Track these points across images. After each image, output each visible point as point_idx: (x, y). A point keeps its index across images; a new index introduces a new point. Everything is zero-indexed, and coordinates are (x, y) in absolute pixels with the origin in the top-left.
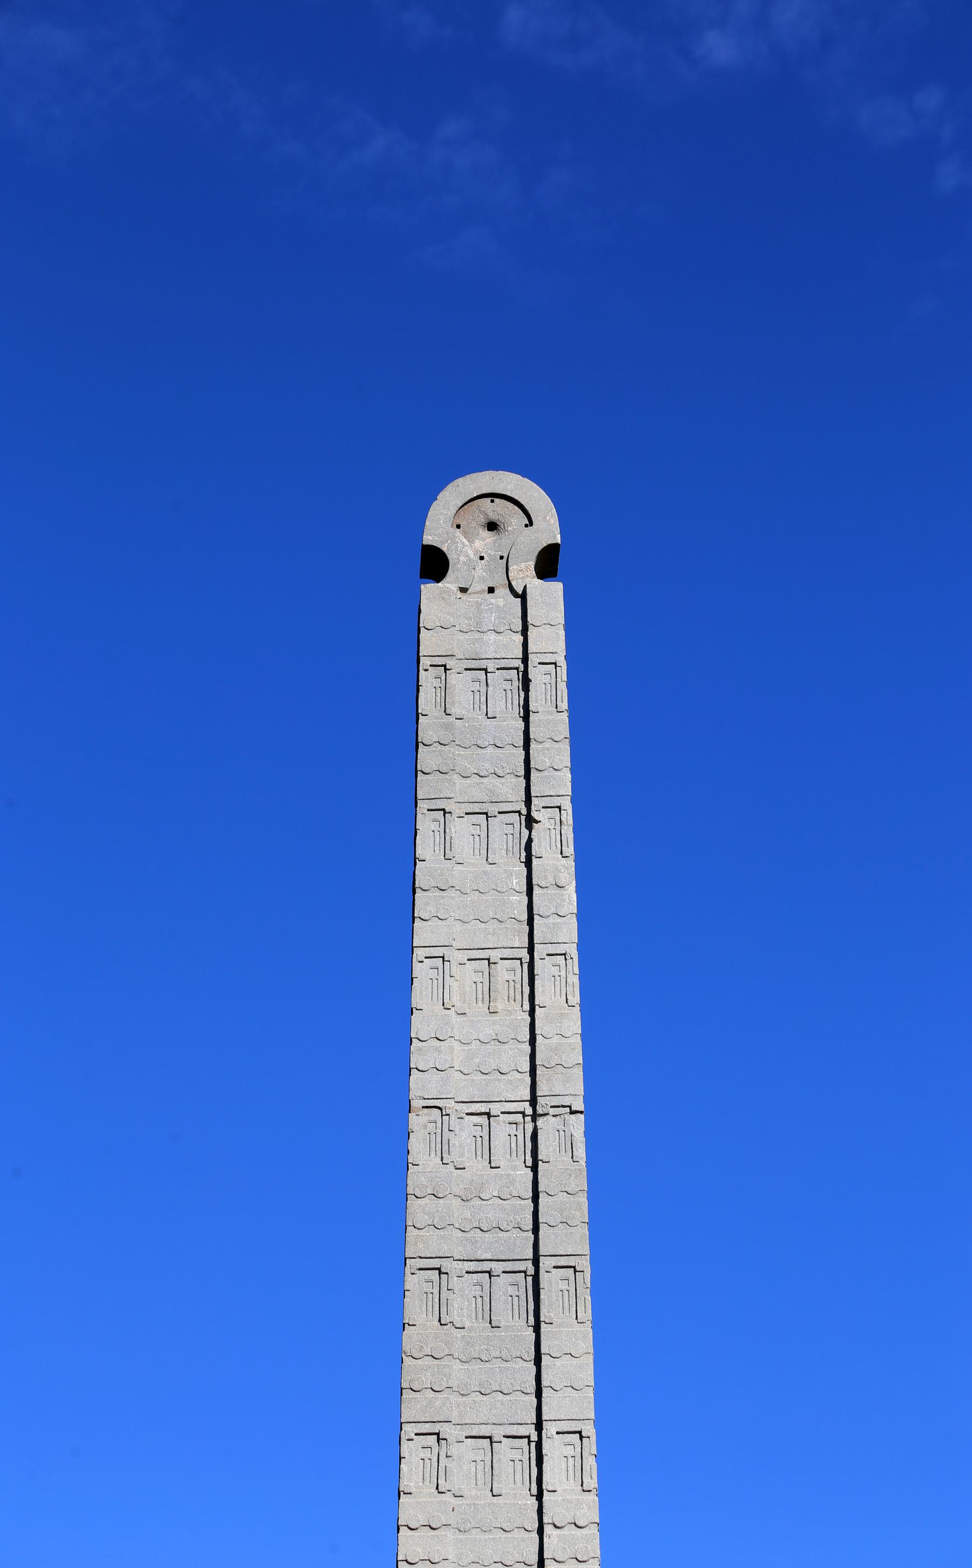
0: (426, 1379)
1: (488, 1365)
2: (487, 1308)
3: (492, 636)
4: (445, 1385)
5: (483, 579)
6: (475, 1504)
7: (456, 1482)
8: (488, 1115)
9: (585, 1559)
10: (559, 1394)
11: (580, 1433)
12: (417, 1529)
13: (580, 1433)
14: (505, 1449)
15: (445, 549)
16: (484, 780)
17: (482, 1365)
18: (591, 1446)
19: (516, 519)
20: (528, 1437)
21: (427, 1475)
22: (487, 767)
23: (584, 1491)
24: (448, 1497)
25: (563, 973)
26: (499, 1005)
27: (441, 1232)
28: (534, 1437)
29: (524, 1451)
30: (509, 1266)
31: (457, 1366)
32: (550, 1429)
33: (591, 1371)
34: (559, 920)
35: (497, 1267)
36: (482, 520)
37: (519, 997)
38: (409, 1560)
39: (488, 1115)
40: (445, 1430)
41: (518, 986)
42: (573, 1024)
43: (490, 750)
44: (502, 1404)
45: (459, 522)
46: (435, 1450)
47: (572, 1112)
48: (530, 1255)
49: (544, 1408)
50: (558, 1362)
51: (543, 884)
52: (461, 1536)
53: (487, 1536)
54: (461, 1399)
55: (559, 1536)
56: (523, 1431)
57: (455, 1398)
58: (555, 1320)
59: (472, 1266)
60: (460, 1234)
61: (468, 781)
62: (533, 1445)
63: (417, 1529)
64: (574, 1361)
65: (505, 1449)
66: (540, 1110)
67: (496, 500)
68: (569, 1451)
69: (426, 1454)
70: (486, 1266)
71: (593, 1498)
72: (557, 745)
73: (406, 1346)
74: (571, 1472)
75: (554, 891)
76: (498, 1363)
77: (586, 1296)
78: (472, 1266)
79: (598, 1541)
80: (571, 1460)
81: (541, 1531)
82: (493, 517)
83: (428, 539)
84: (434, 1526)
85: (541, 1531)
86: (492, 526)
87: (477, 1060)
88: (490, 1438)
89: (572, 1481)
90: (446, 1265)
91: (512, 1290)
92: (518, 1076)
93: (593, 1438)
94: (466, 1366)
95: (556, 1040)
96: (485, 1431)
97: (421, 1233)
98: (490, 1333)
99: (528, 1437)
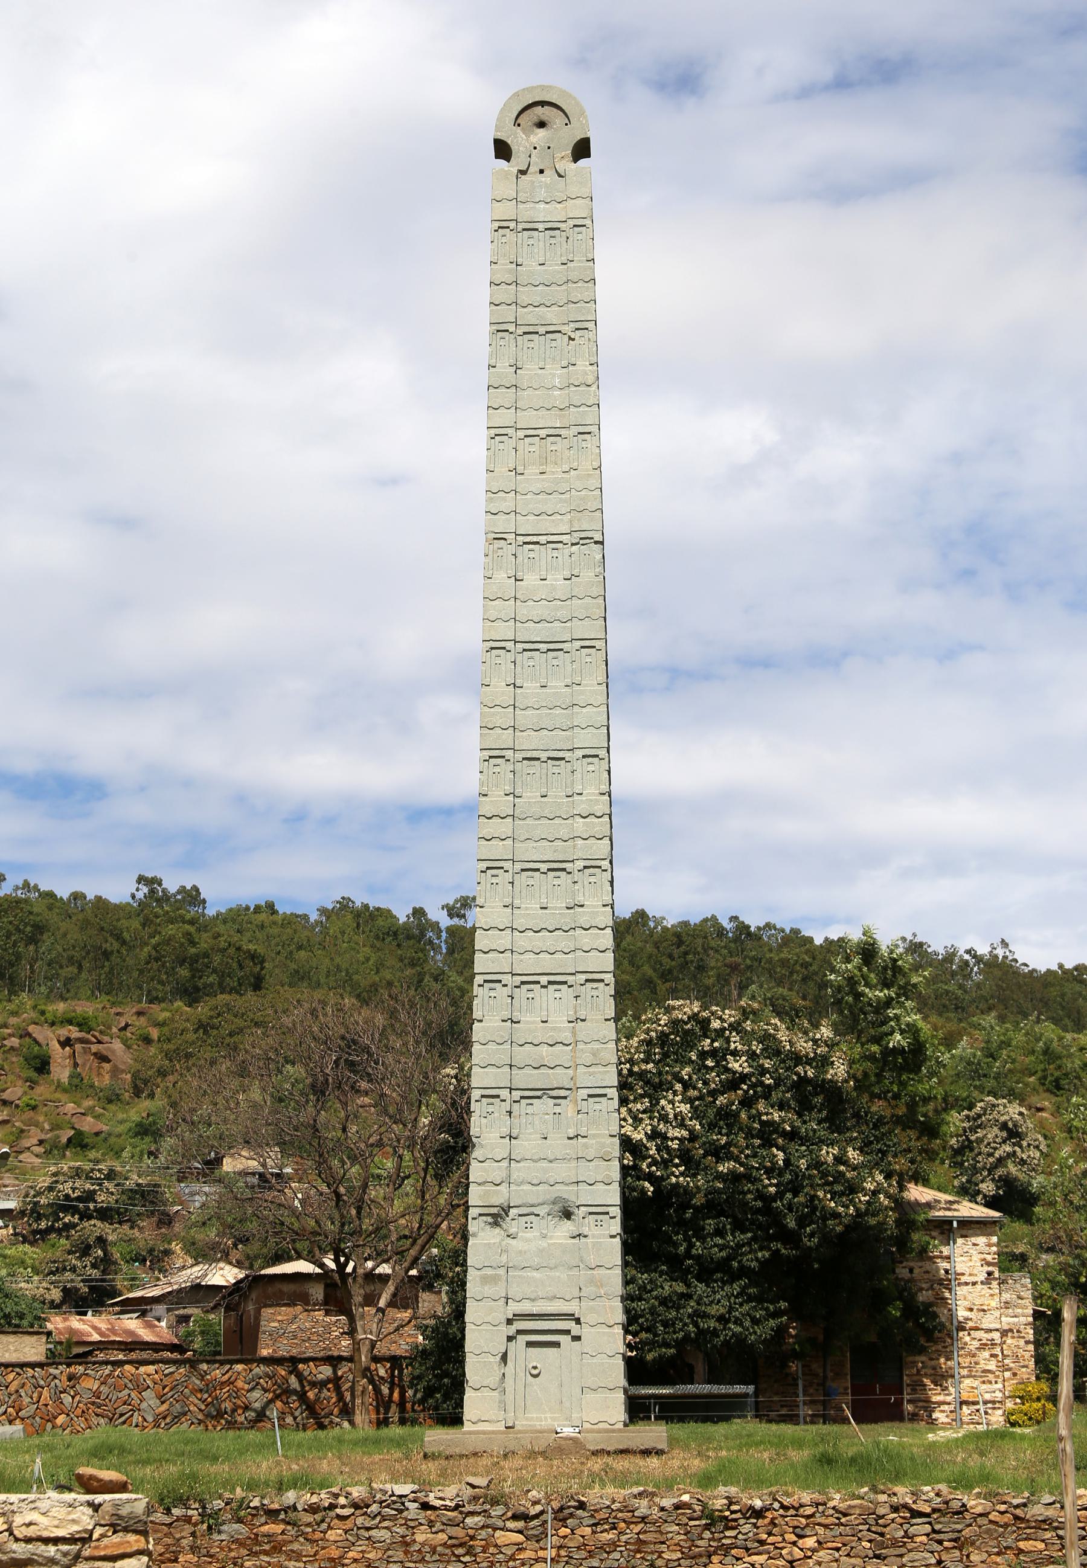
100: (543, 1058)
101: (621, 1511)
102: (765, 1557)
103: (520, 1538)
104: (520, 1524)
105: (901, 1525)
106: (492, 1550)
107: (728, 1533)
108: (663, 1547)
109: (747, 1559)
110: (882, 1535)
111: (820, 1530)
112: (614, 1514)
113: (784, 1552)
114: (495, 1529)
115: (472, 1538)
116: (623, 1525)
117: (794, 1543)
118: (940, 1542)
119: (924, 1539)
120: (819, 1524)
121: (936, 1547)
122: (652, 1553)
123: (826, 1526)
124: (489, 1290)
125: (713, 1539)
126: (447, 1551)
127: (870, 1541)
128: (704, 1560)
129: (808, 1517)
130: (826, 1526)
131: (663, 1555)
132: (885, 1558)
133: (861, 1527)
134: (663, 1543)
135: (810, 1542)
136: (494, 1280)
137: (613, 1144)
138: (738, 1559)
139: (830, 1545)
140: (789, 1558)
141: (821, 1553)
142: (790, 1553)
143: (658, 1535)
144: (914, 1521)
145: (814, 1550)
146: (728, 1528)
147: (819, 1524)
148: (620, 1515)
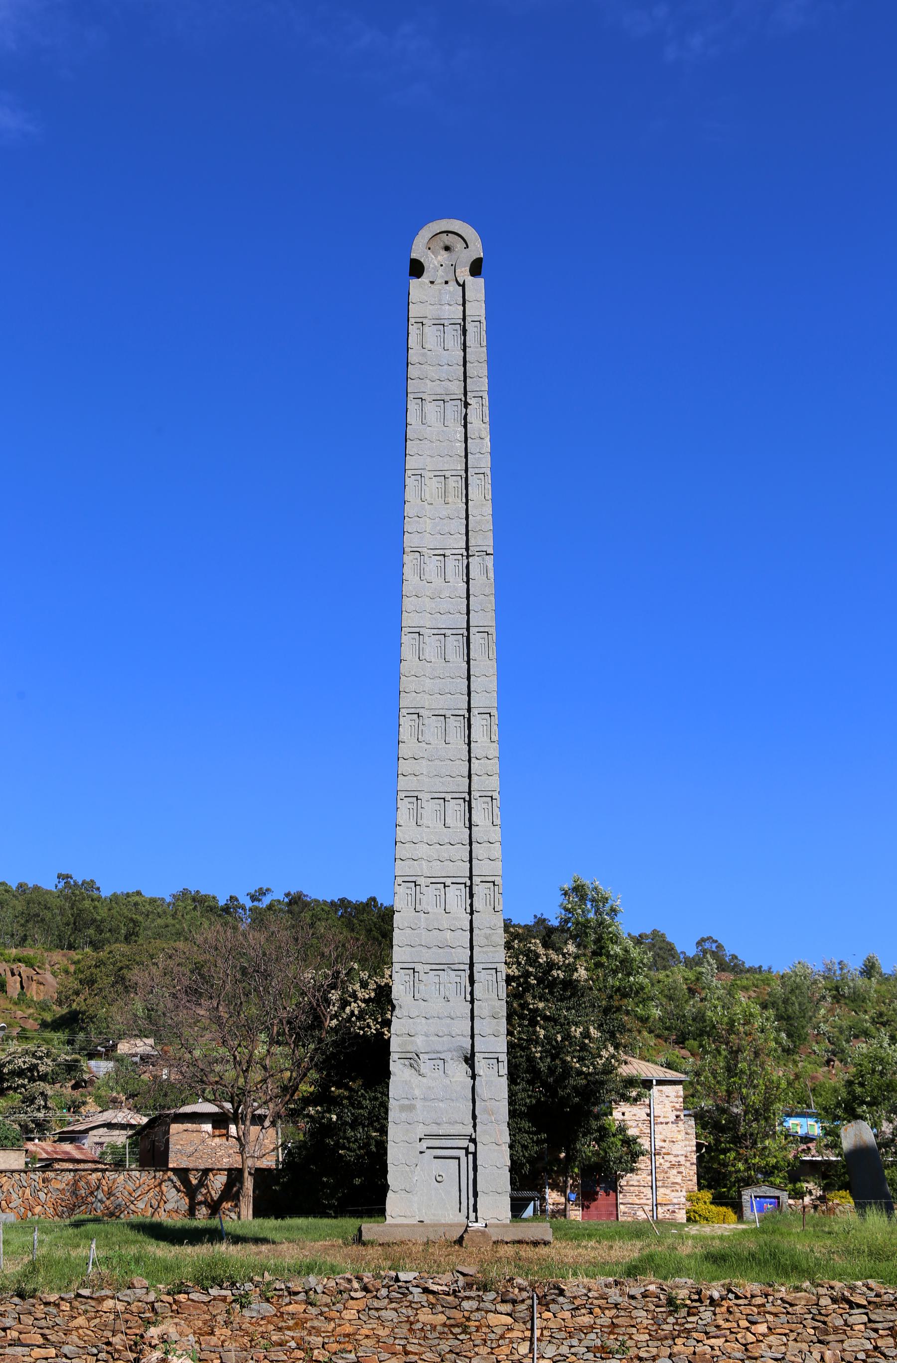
0: (412, 687)
1: (443, 680)
2: (443, 652)
3: (447, 307)
4: (421, 690)
5: (442, 277)
7: (427, 737)
8: (444, 556)
10: (479, 695)
11: (490, 714)
13: (490, 714)
14: (452, 721)
15: (422, 261)
16: (442, 383)
17: (441, 680)
18: (495, 720)
19: (459, 245)
20: (464, 716)
22: (444, 376)
24: (423, 744)
25: (483, 483)
26: (450, 500)
27: (420, 614)
28: (467, 716)
29: (461, 723)
30: (455, 632)
31: (428, 680)
32: (474, 712)
33: (496, 684)
34: (481, 456)
35: (448, 632)
36: (442, 245)
37: (460, 495)
39: (444, 556)
40: (422, 712)
41: (460, 490)
42: (488, 509)
43: (446, 367)
44: (451, 699)
45: (430, 246)
46: (417, 721)
47: (487, 554)
48: (465, 626)
49: (472, 702)
50: (479, 679)
51: (473, 437)
52: (430, 763)
53: (442, 763)
54: (430, 697)
55: (479, 763)
56: (461, 713)
57: (427, 696)
58: (477, 659)
59: (436, 631)
60: (430, 615)
61: (434, 383)
62: (466, 719)
64: (487, 679)
65: (452, 721)
66: (470, 553)
67: (449, 234)
68: (484, 722)
69: (413, 723)
70: (443, 631)
71: (496, 745)
72: (480, 365)
73: (402, 671)
74: (485, 732)
75: (478, 441)
76: (449, 680)
77: (493, 647)
78: (436, 631)
80: (485, 727)
81: (469, 761)
82: (447, 243)
83: (414, 255)
85: (469, 761)
86: (447, 248)
87: (438, 528)
88: (444, 716)
90: (422, 631)
91: (455, 643)
92: (460, 536)
93: (496, 716)
94: (432, 681)
95: (479, 517)
96: (442, 712)
97: (410, 615)
98: (444, 664)
99: (464, 716)
100: (447, 940)
101: (596, 1298)
102: (723, 1340)
103: (509, 1320)
104: (507, 1308)
105: (841, 1315)
106: (484, 1330)
107: (690, 1319)
108: (634, 1330)
109: (706, 1342)
110: (824, 1323)
111: (770, 1318)
112: (590, 1301)
113: (739, 1336)
114: (487, 1312)
115: (468, 1319)
116: (597, 1310)
117: (747, 1328)
118: (876, 1330)
119: (862, 1327)
120: (769, 1313)
121: (873, 1335)
122: (624, 1334)
123: (776, 1315)
124: (404, 1116)
125: (676, 1324)
126: (446, 1330)
127: (814, 1328)
128: (670, 1342)
129: (759, 1306)
130: (776, 1315)
131: (633, 1336)
132: (828, 1343)
133: (806, 1316)
134: (633, 1326)
135: (762, 1328)
137: (501, 1006)
138: (698, 1341)
139: (778, 1331)
140: (744, 1342)
141: (772, 1338)
142: (744, 1337)
143: (628, 1319)
144: (853, 1311)
145: (764, 1335)
146: (689, 1314)
147: (769, 1313)
148: (595, 1302)
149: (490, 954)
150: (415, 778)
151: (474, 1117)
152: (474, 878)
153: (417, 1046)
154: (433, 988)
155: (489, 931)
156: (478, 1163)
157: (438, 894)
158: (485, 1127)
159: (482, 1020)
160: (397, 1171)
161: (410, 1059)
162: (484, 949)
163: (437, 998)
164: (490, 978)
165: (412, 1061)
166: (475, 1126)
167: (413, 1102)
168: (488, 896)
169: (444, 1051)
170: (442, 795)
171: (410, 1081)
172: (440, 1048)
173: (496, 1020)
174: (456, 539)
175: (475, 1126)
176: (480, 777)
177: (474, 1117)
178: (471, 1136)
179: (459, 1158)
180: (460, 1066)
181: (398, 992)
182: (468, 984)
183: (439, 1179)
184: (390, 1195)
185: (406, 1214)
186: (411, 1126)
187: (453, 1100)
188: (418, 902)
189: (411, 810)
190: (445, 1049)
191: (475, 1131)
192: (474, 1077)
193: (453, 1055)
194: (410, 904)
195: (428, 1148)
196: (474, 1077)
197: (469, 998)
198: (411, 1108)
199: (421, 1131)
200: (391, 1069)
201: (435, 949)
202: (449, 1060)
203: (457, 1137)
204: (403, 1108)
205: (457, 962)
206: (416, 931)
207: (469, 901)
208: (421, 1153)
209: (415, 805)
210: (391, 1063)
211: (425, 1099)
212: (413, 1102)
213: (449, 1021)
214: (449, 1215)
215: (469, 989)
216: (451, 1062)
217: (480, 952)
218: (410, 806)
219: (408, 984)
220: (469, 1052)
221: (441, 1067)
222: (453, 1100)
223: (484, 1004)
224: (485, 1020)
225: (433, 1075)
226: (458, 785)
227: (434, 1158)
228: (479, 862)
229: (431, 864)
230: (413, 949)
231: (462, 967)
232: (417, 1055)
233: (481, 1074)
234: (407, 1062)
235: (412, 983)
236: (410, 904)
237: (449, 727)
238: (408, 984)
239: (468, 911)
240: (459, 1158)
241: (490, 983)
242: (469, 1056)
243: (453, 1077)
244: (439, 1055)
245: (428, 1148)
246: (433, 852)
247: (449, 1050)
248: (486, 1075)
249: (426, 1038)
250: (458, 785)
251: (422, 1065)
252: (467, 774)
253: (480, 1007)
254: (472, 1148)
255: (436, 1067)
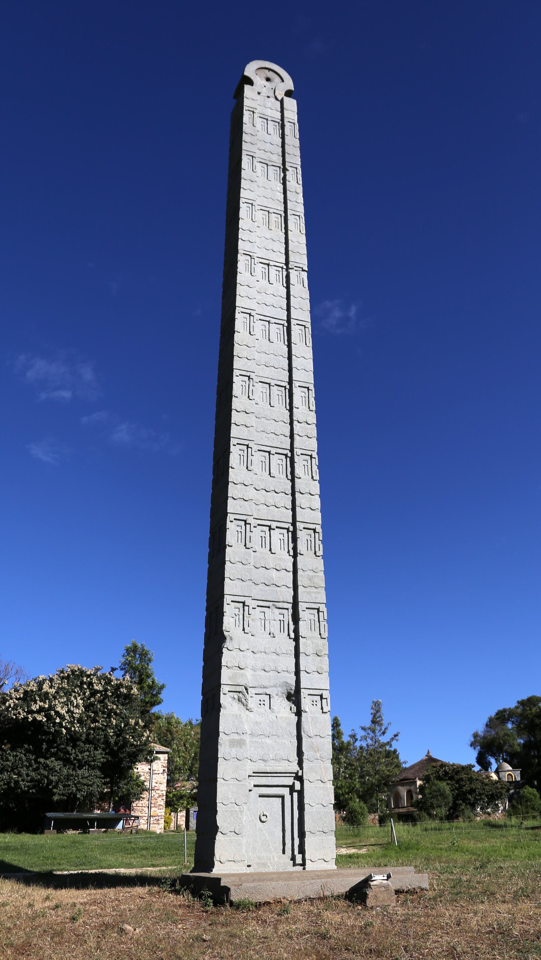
2: (267, 335)
6: (263, 408)
9: (311, 437)
12: (240, 412)
21: (244, 392)
23: (310, 410)
25: (298, 222)
30: (277, 321)
32: (295, 384)
35: (273, 321)
37: (280, 227)
38: (237, 424)
41: (280, 224)
42: (303, 239)
53: (268, 422)
55: (300, 426)
59: (262, 318)
63: (240, 412)
66: (290, 266)
79: (316, 431)
84: (247, 412)
89: (304, 406)
93: (313, 391)
100: (273, 579)
124: (234, 752)
136: (240, 743)
137: (324, 645)
149: (313, 595)
150: (246, 429)
151: (300, 753)
152: (298, 524)
153: (247, 679)
154: (259, 623)
155: (311, 574)
156: (306, 801)
157: (263, 535)
158: (311, 764)
159: (307, 657)
160: (226, 811)
161: (239, 692)
162: (308, 590)
163: (262, 634)
164: (312, 617)
165: (241, 695)
166: (300, 764)
167: (243, 737)
168: (309, 542)
169: (271, 687)
170: (268, 449)
171: (240, 715)
172: (266, 683)
173: (319, 658)
174: (277, 255)
175: (300, 764)
176: (301, 438)
177: (300, 753)
178: (297, 773)
179: (283, 797)
180: (283, 702)
181: (228, 624)
182: (291, 623)
183: (263, 819)
184: (219, 836)
185: (235, 859)
186: (241, 762)
187: (278, 736)
188: (248, 539)
189: (242, 457)
190: (272, 685)
191: (301, 768)
192: (299, 713)
193: (278, 691)
194: (240, 541)
195: (255, 786)
196: (299, 713)
197: (292, 635)
198: (240, 743)
199: (250, 768)
200: (222, 701)
201: (262, 586)
202: (275, 695)
203: (283, 775)
204: (234, 743)
205: (281, 600)
206: (246, 566)
207: (291, 545)
208: (250, 791)
209: (246, 452)
210: (222, 696)
211: (252, 734)
212: (243, 737)
213: (275, 656)
214: (273, 857)
215: (292, 627)
216: (276, 697)
217: (304, 592)
218: (241, 453)
219: (238, 617)
220: (293, 688)
221: (267, 703)
222: (278, 736)
223: (309, 642)
224: (309, 657)
225: (259, 710)
226: (281, 442)
227: (260, 796)
228: (302, 510)
229: (258, 507)
230: (244, 583)
231: (286, 605)
232: (246, 689)
233: (307, 710)
234: (236, 695)
235: (241, 617)
236: (240, 541)
237: (273, 393)
238: (238, 617)
239: (292, 553)
240: (283, 797)
241: (313, 623)
242: (292, 692)
243: (278, 712)
244: (265, 690)
245: (255, 786)
246: (260, 496)
247: (275, 686)
248: (311, 712)
249: (253, 673)
250: (281, 442)
251: (249, 699)
252: (288, 434)
253: (305, 644)
254: (298, 786)
255: (262, 703)
